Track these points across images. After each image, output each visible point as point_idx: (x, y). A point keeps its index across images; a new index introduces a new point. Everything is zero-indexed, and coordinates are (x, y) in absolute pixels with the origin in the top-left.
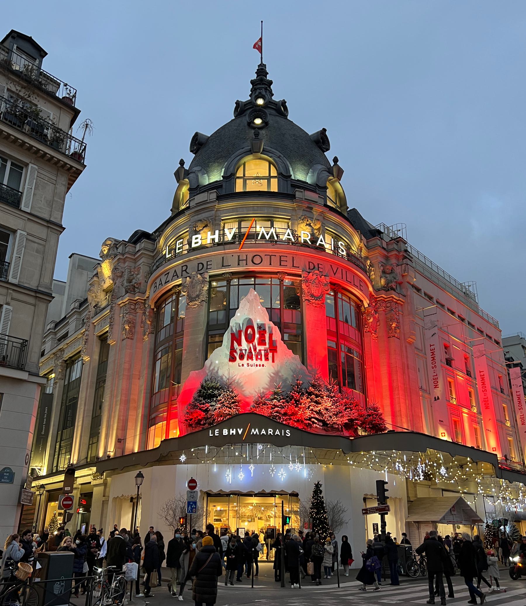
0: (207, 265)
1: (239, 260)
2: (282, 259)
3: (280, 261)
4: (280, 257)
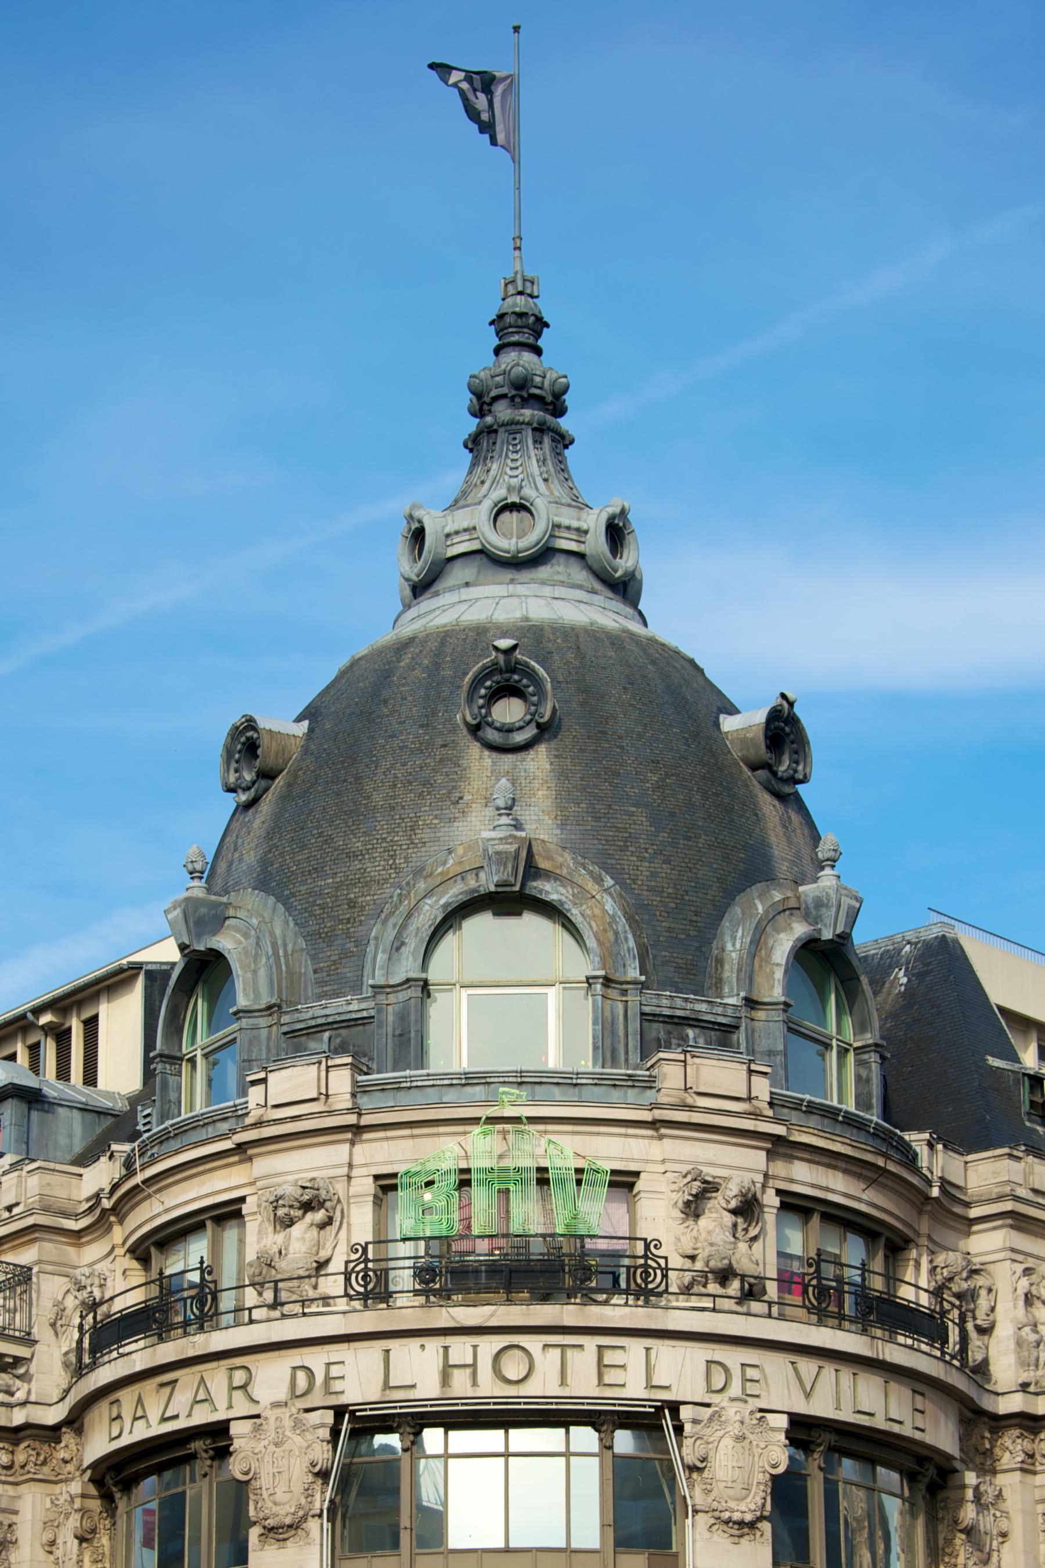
3: (601, 1366)
4: (599, 1347)
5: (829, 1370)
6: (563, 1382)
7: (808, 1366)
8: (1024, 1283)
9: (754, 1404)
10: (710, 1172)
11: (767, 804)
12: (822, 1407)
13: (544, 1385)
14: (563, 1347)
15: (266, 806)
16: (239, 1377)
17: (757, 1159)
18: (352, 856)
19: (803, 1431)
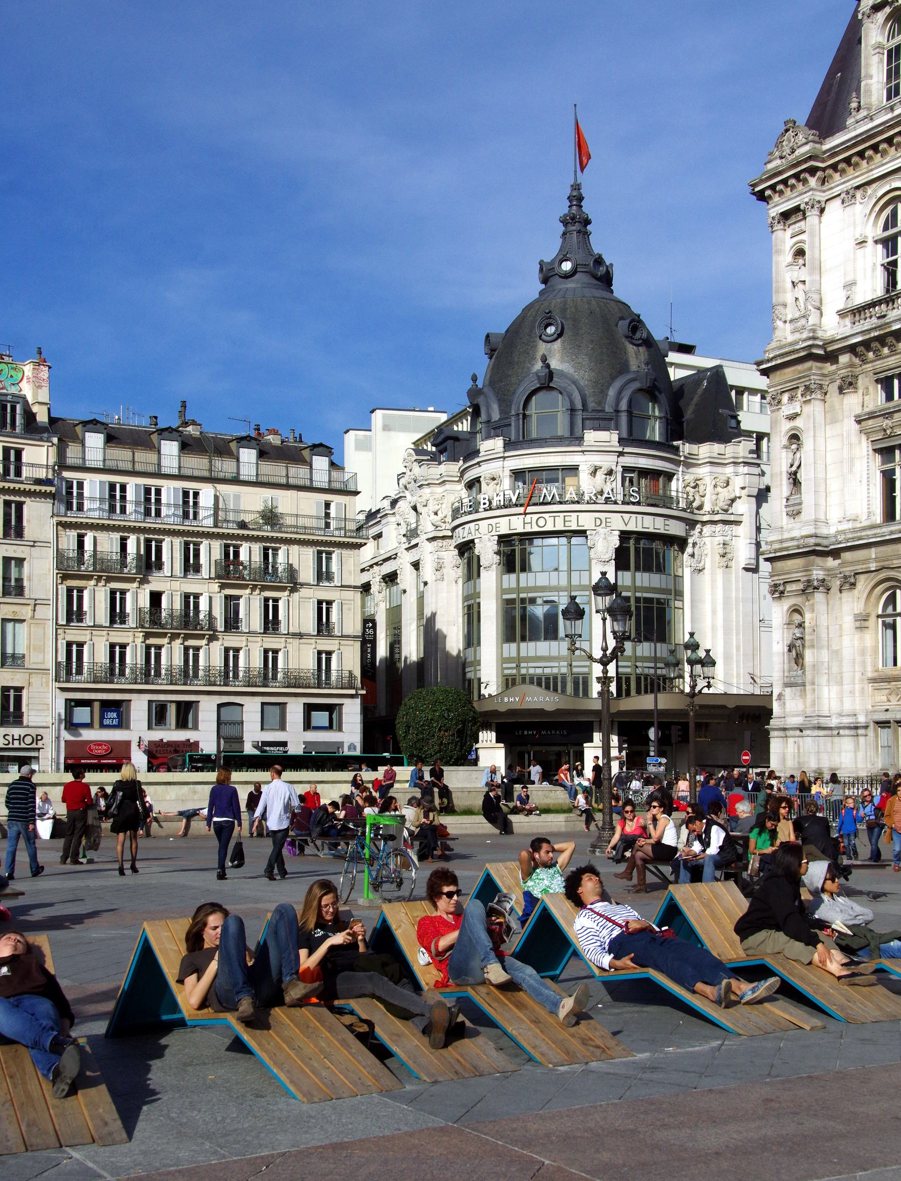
2: (567, 519)
8: (714, 483)
9: (609, 529)
10: (598, 464)
12: (631, 527)
13: (549, 527)
17: (614, 458)
18: (509, 376)
19: (625, 536)
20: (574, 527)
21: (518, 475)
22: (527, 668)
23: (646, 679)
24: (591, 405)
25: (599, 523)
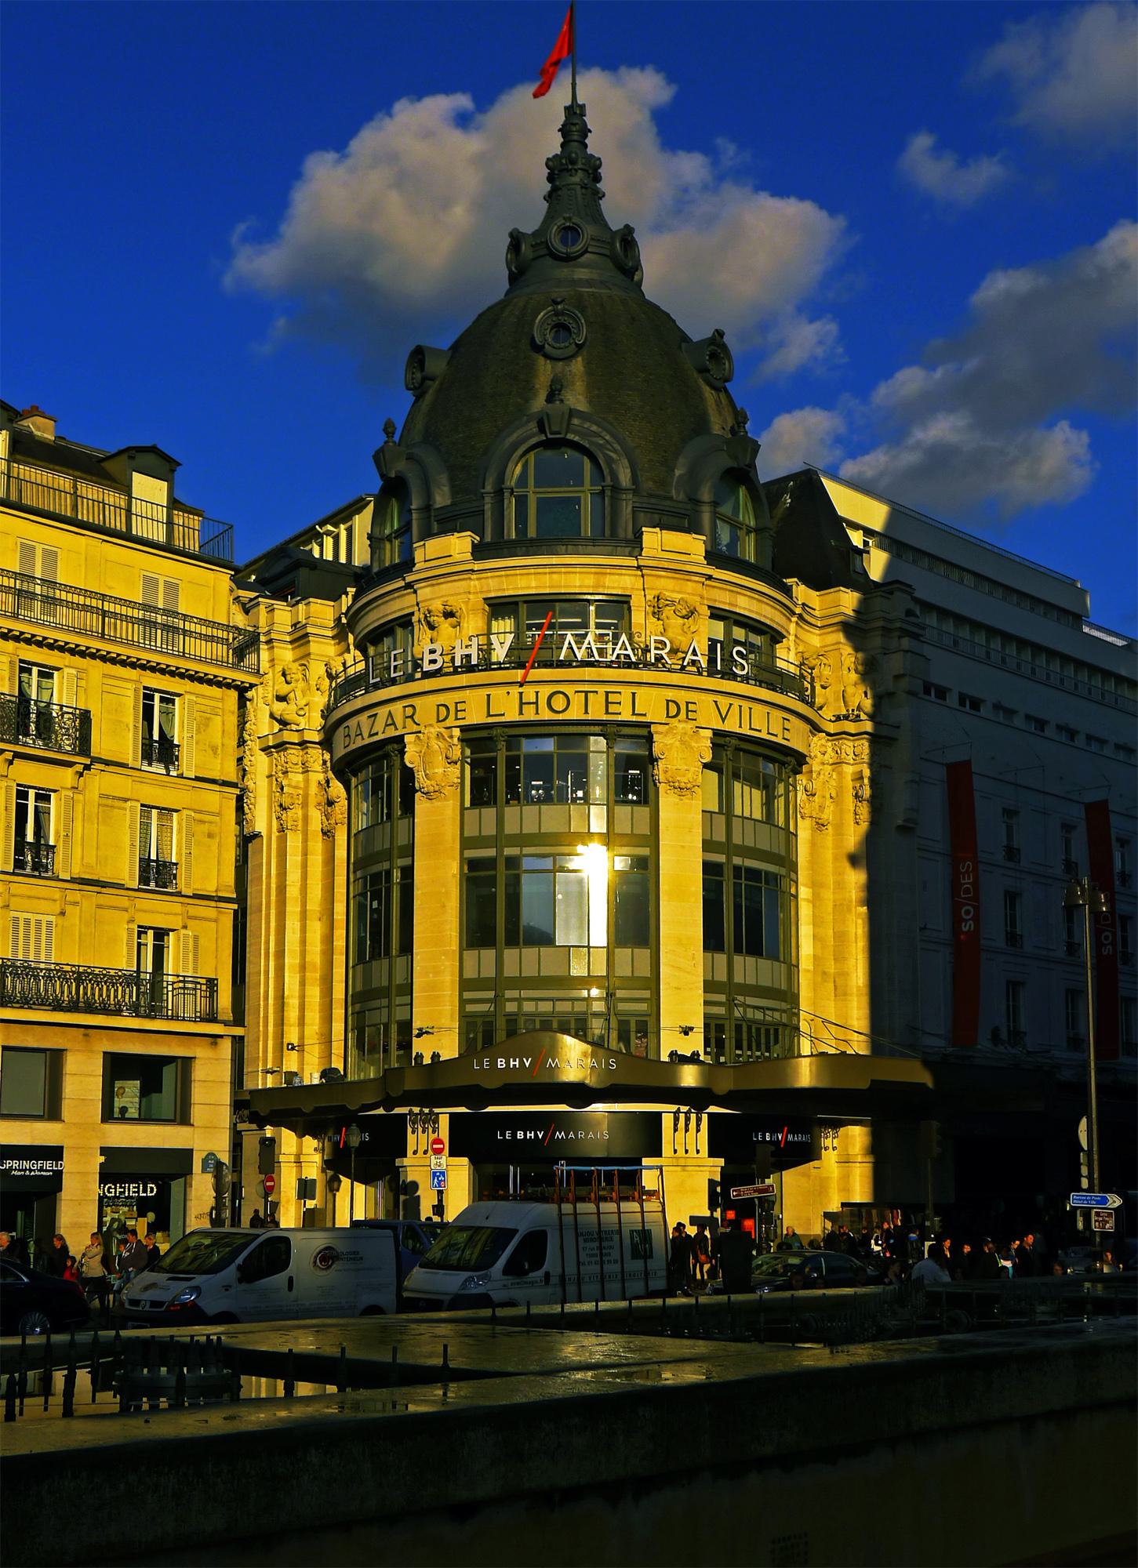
0: (457, 711)
1: (521, 704)
2: (611, 698)
3: (607, 703)
4: (607, 693)
5: (736, 702)
6: (586, 712)
7: (724, 702)
9: (692, 724)
11: (708, 393)
12: (731, 725)
14: (586, 693)
15: (429, 398)
16: (409, 711)
20: (626, 716)
21: (499, 607)
22: (519, 1000)
23: (749, 1028)
24: (648, 485)
25: (674, 711)
